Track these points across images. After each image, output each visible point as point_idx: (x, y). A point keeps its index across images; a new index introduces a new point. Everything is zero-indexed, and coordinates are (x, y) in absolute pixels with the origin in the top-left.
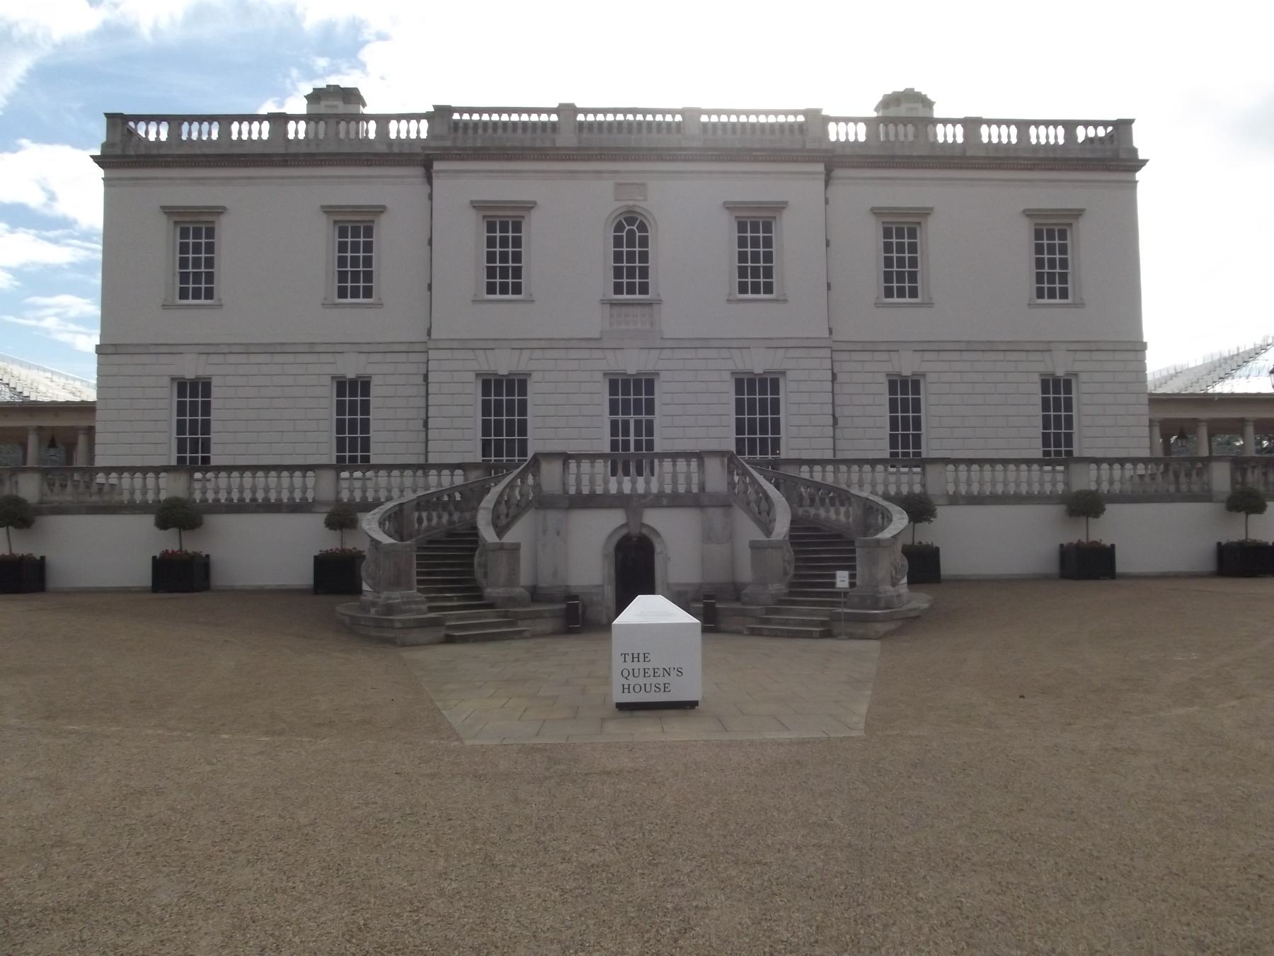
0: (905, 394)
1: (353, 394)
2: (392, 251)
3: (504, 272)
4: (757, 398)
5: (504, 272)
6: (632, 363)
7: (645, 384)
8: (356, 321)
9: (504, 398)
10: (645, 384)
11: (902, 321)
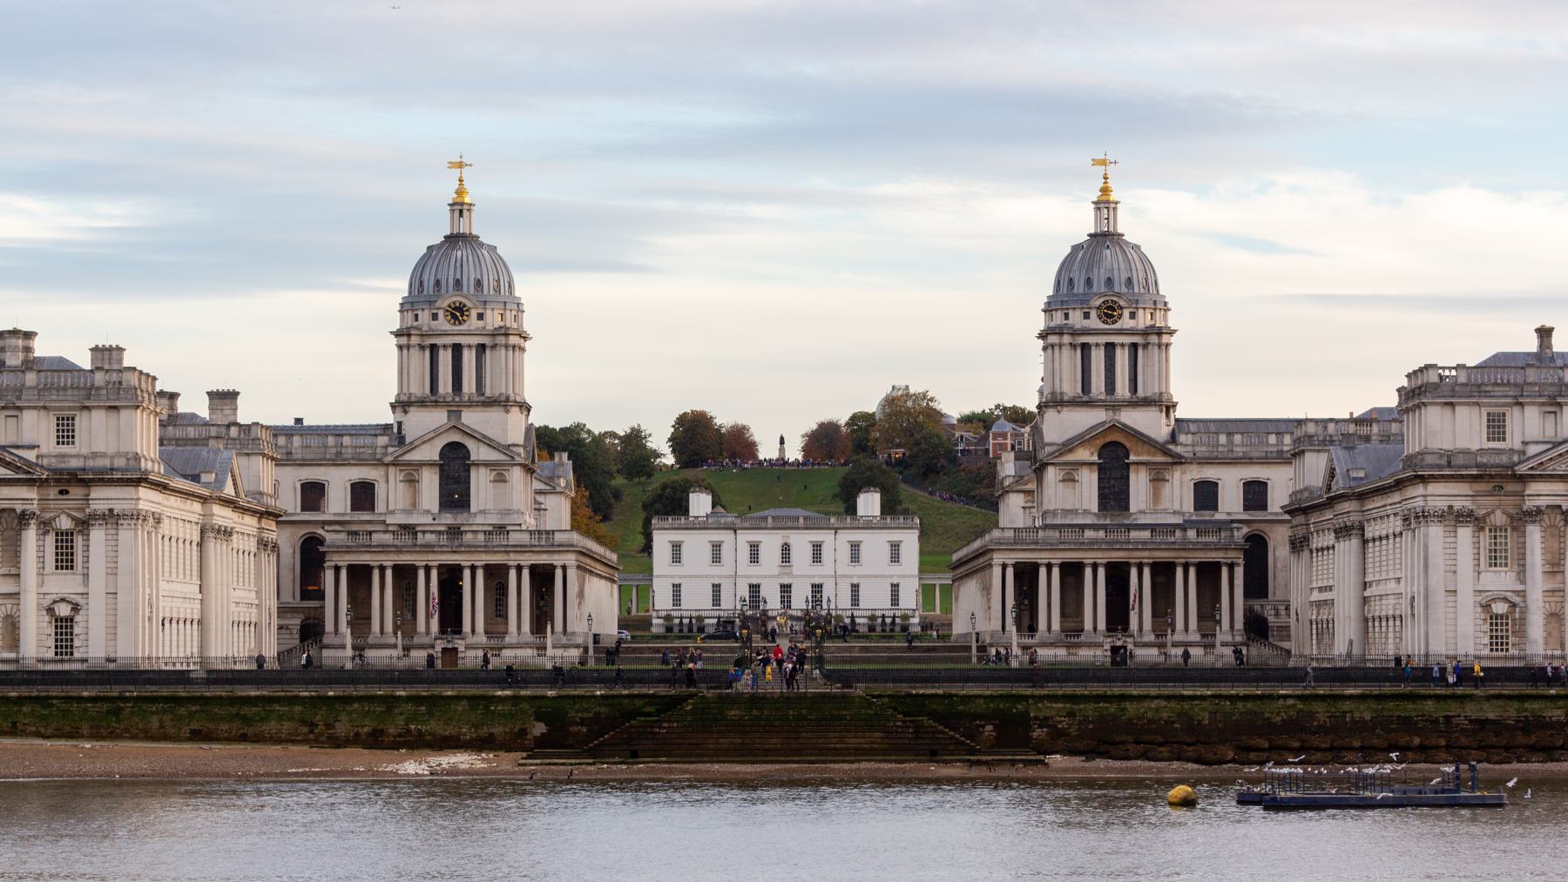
0: (855, 588)
1: (716, 588)
2: (726, 552)
3: (754, 557)
4: (817, 588)
5: (754, 557)
6: (786, 581)
7: (789, 586)
8: (716, 570)
9: (755, 589)
10: (789, 586)
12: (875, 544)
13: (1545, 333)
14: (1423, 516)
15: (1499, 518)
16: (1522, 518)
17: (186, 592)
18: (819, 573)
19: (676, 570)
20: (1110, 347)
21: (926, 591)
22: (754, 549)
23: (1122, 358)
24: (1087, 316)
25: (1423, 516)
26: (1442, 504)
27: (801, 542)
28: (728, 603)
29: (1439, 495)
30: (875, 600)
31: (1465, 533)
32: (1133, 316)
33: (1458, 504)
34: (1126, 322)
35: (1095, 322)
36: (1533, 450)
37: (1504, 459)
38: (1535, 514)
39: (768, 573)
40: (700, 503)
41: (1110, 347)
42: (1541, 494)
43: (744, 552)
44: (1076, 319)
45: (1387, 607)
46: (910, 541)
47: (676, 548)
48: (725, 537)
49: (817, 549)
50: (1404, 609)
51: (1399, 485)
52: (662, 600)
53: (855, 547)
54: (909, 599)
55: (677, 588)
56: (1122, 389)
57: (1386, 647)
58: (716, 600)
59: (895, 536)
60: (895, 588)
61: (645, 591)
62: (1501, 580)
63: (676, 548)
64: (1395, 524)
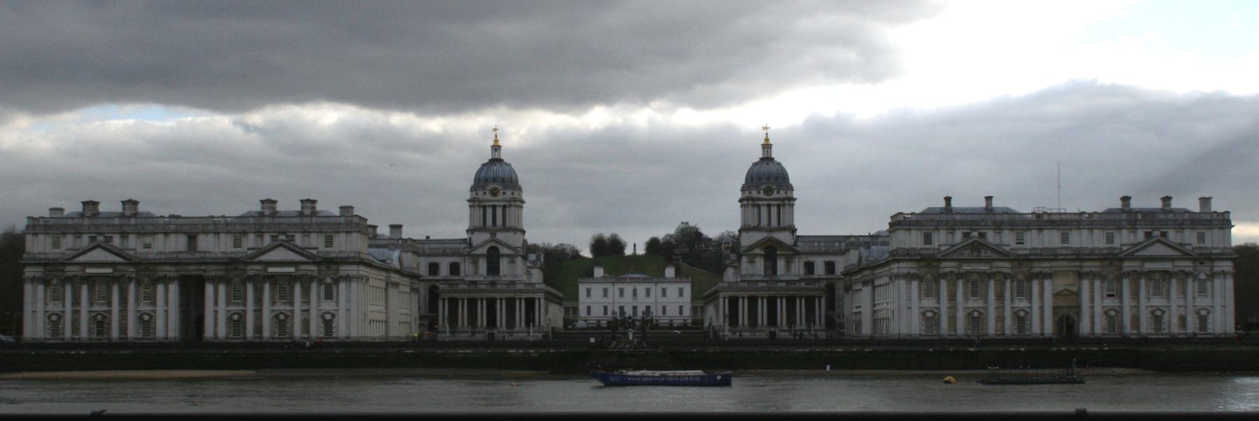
0: (664, 308)
3: (622, 294)
4: (648, 308)
5: (622, 294)
8: (605, 300)
9: (622, 308)
11: (664, 300)
12: (672, 289)
13: (948, 199)
14: (898, 276)
15: (929, 277)
16: (938, 277)
17: (370, 311)
18: (650, 301)
19: (588, 300)
21: (694, 309)
22: (621, 291)
25: (898, 276)
26: (906, 271)
27: (641, 288)
28: (610, 313)
29: (904, 267)
30: (673, 312)
31: (915, 284)
33: (912, 271)
36: (943, 248)
37: (931, 252)
38: (944, 276)
39: (628, 299)
40: (599, 272)
42: (947, 267)
43: (617, 293)
45: (882, 314)
46: (687, 288)
47: (589, 291)
48: (609, 286)
49: (648, 291)
50: (890, 315)
51: (888, 263)
52: (583, 312)
53: (664, 291)
54: (687, 312)
55: (589, 308)
57: (883, 331)
58: (606, 313)
59: (681, 285)
60: (681, 308)
61: (576, 310)
62: (929, 303)
63: (589, 291)
64: (886, 280)
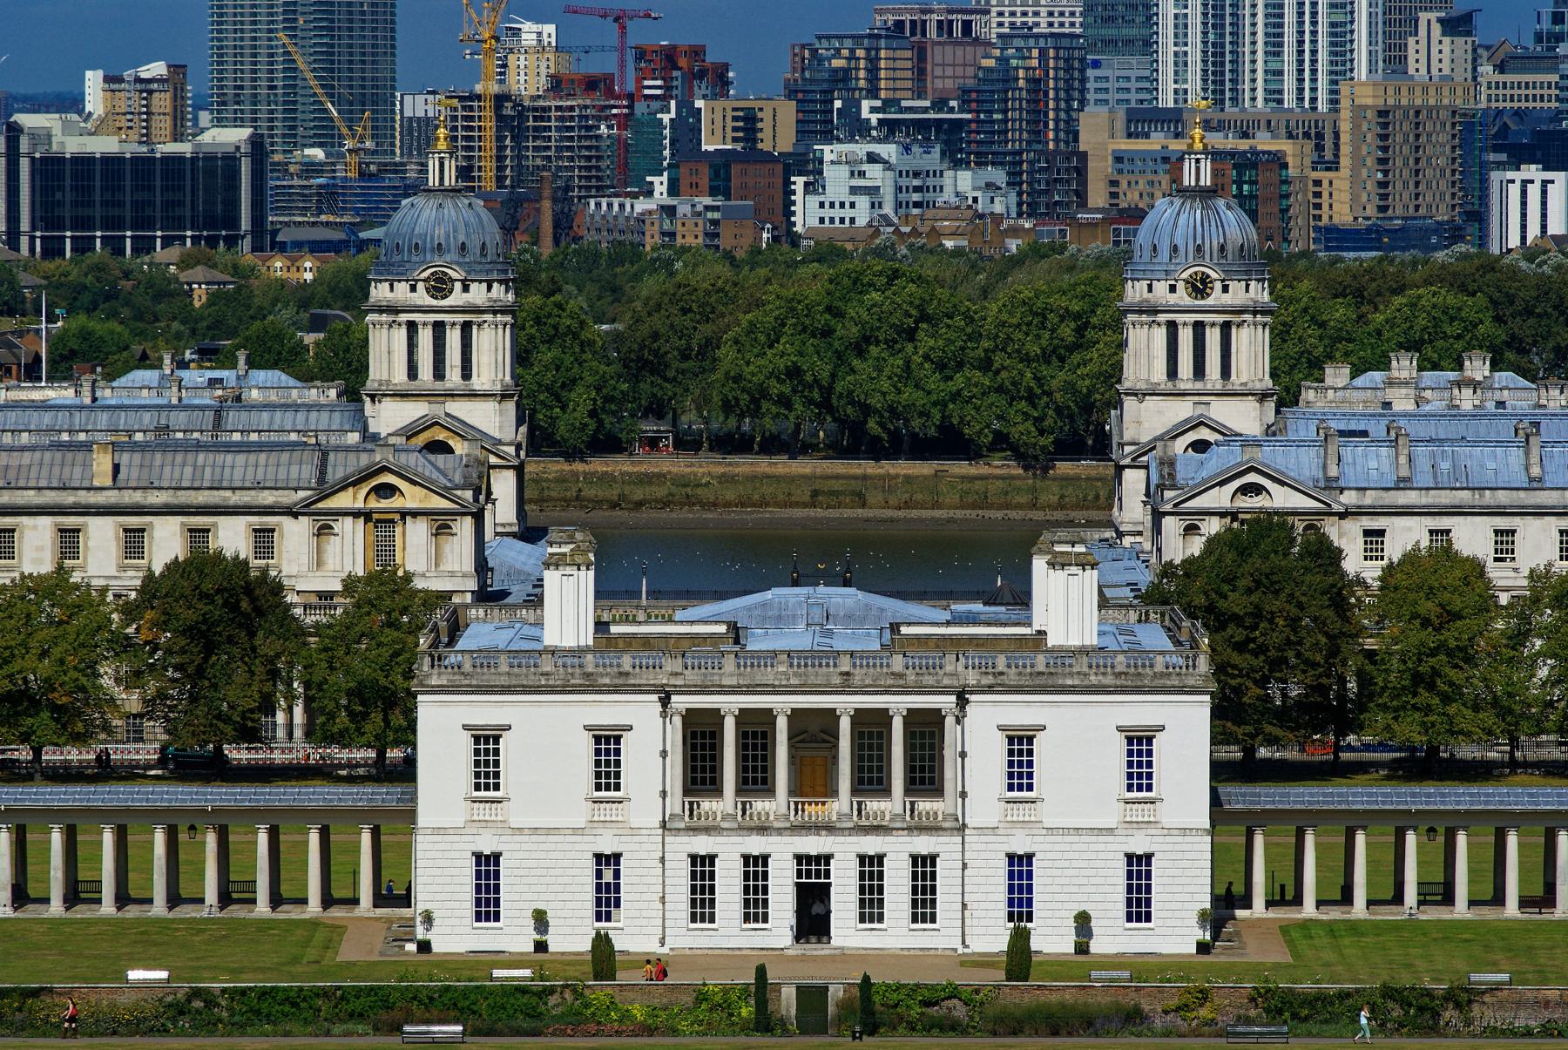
20: (439, 327)
23: (453, 338)
24: (413, 289)
32: (466, 289)
34: (457, 298)
35: (422, 297)
41: (439, 327)
44: (401, 293)
56: (453, 376)
